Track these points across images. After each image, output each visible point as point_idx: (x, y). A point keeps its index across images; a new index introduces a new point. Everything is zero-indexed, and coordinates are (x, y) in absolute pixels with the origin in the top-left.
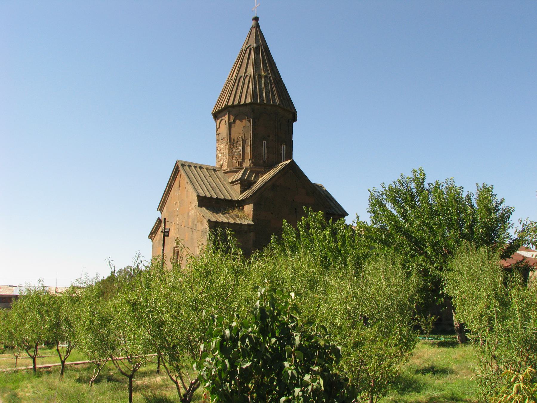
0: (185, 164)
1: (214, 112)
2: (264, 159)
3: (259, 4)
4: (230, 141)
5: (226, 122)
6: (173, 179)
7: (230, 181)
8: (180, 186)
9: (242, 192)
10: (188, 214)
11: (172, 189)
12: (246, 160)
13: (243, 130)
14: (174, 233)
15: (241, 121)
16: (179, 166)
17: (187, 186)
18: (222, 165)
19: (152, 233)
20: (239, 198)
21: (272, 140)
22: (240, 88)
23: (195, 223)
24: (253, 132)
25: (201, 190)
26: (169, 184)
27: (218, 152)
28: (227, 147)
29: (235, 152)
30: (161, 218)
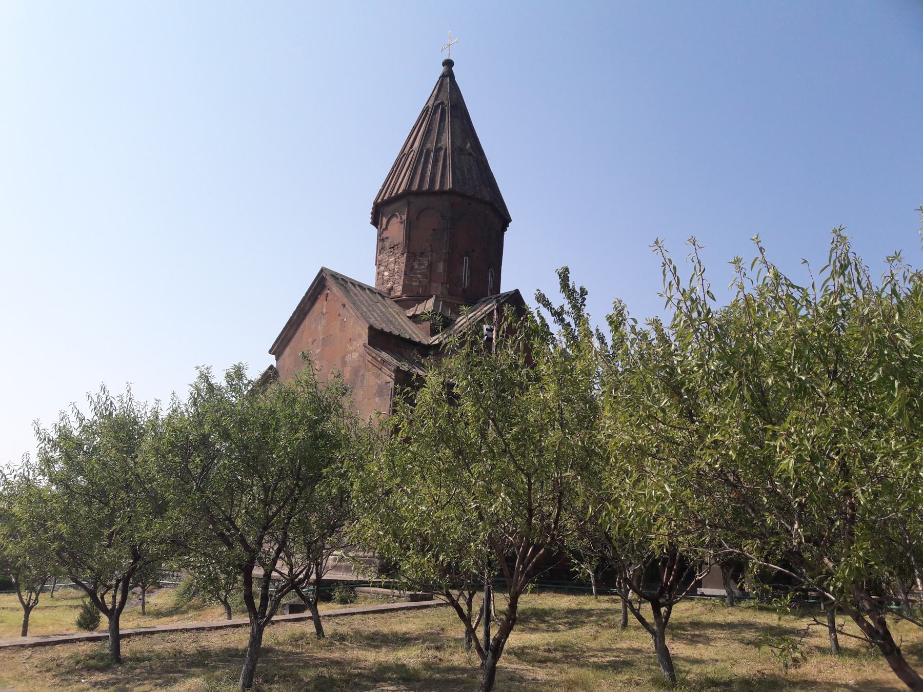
0: (337, 276)
1: (379, 200)
7: (411, 314)
9: (434, 332)
10: (344, 357)
13: (432, 235)
16: (328, 278)
17: (341, 311)
18: (391, 289)
20: (430, 342)
21: (478, 257)
23: (361, 373)
25: (373, 319)
27: (382, 268)
28: (403, 259)
30: (275, 366)
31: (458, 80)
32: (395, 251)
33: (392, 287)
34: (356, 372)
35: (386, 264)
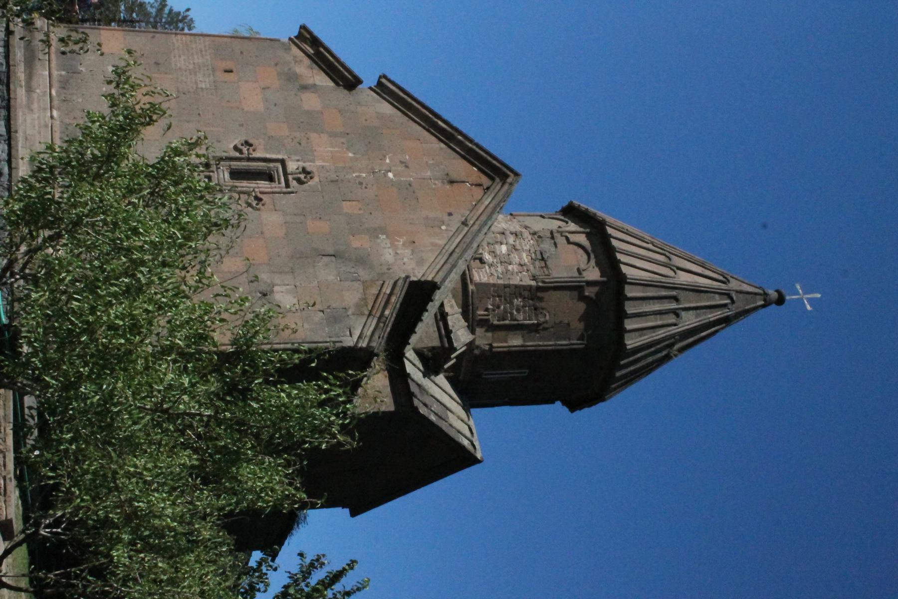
2: (486, 375)
3: (809, 307)
4: (538, 289)
5: (584, 270)
6: (470, 151)
7: (447, 309)
8: (452, 182)
9: (419, 353)
10: (383, 230)
11: (443, 145)
12: (490, 334)
13: (561, 322)
14: (324, 161)
15: (580, 320)
16: (506, 187)
19: (318, 47)
22: (657, 307)
24: (553, 351)
26: (456, 134)
27: (511, 239)
29: (511, 303)
30: (360, 86)
31: (762, 311)
32: (537, 263)
33: (484, 263)
34: (362, 260)
35: (518, 247)
